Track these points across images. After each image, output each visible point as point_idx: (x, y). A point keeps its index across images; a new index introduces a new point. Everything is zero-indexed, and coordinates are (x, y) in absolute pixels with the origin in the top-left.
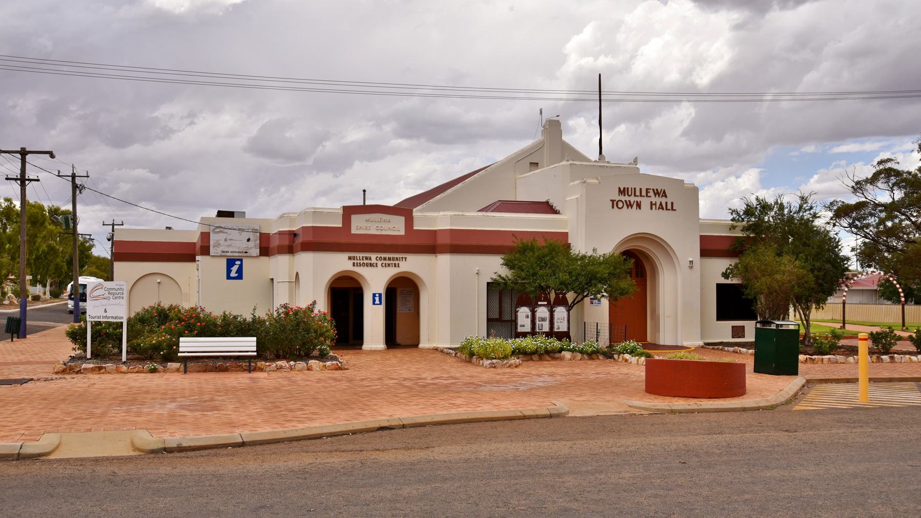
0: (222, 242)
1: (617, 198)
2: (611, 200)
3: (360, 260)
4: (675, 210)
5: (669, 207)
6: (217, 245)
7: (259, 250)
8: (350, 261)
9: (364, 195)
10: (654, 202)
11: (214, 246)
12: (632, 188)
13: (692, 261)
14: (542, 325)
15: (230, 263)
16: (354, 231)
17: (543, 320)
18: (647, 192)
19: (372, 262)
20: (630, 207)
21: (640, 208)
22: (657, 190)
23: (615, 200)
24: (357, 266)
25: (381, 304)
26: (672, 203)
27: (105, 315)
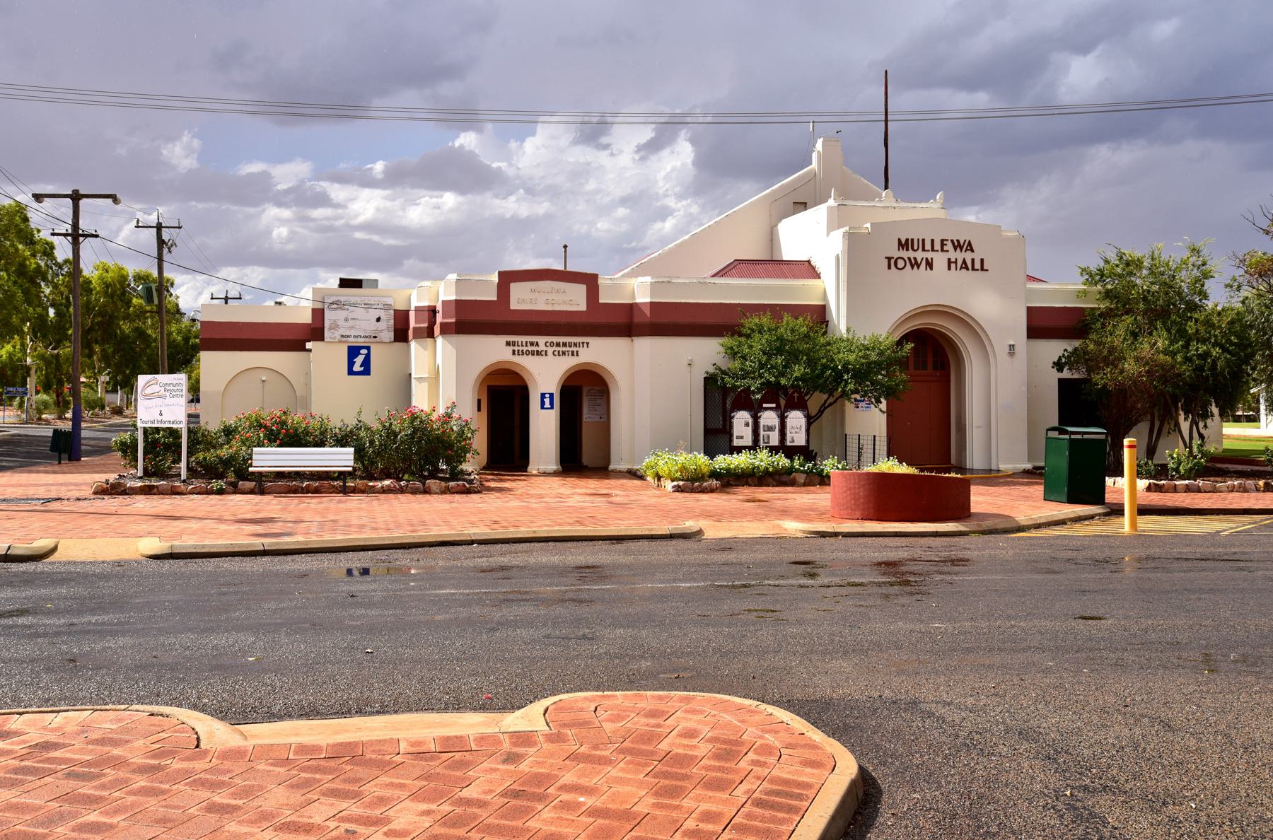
0: (341, 323)
1: (896, 253)
2: (886, 258)
3: (522, 346)
4: (987, 270)
5: (977, 265)
6: (335, 327)
7: (393, 333)
8: (508, 347)
9: (565, 252)
10: (953, 260)
11: (330, 329)
12: (918, 240)
13: (1013, 345)
14: (769, 437)
15: (353, 352)
16: (514, 305)
17: (770, 429)
19: (540, 349)
20: (915, 267)
21: (931, 269)
22: (958, 241)
23: (893, 258)
24: (519, 355)
25: (552, 408)
26: (982, 261)
27: (160, 418)
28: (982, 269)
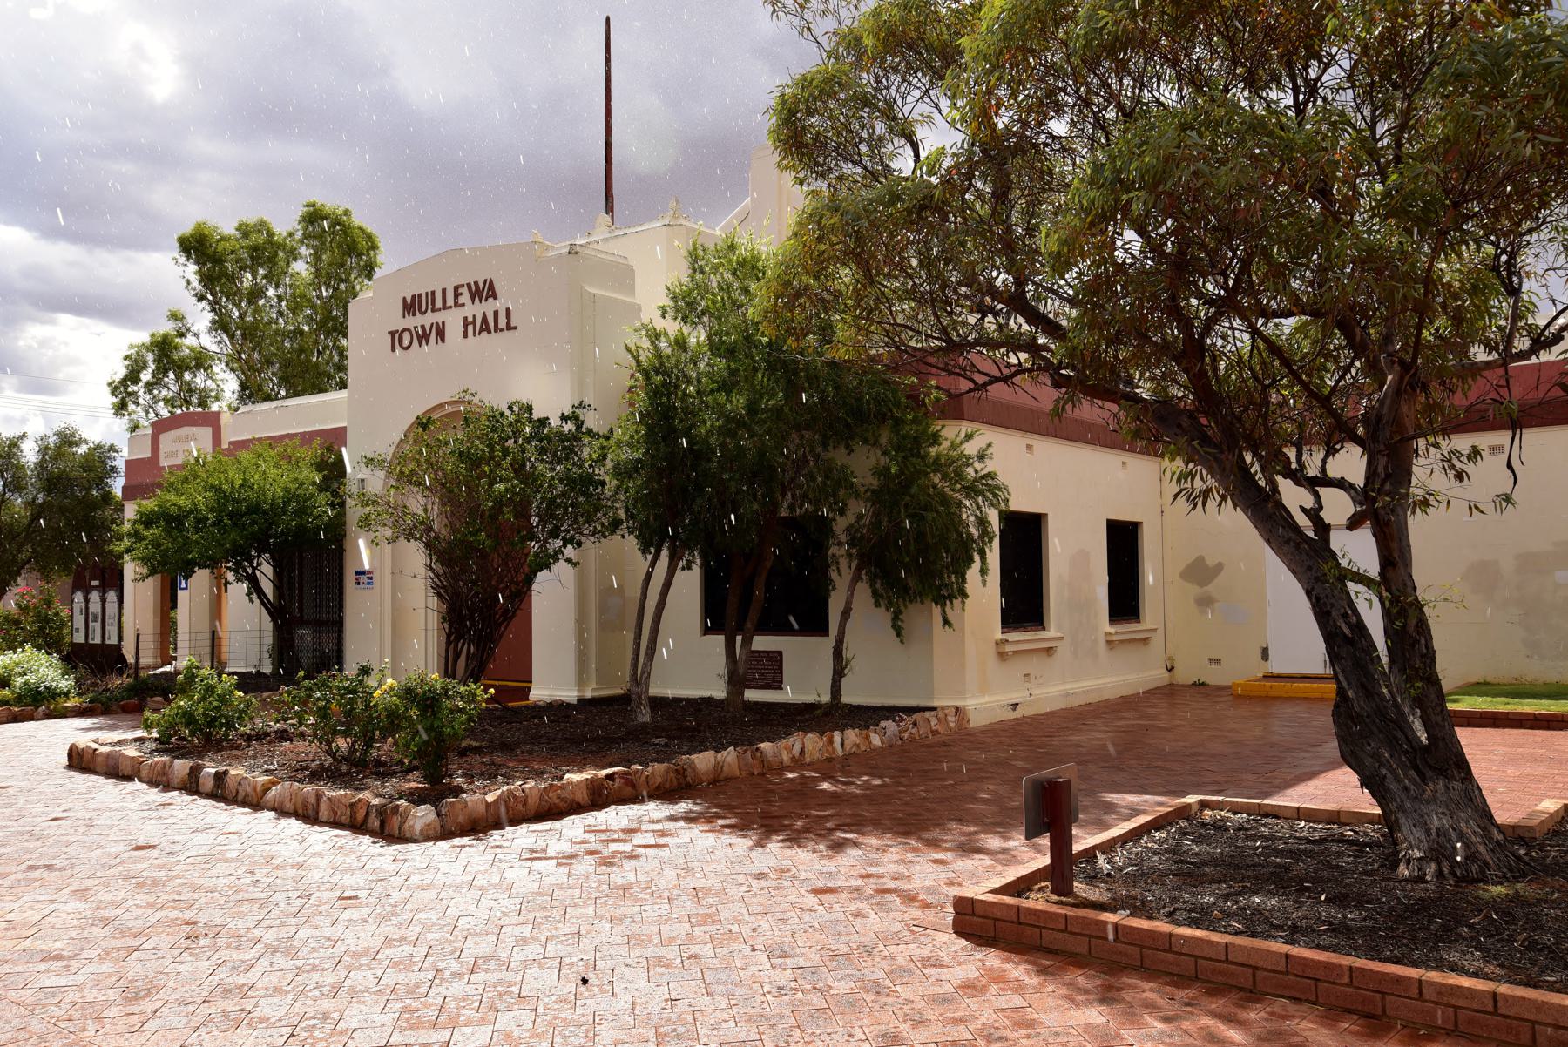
1: (400, 322)
5: (502, 323)
18: (457, 295)
21: (443, 341)
22: (476, 283)
28: (509, 327)
